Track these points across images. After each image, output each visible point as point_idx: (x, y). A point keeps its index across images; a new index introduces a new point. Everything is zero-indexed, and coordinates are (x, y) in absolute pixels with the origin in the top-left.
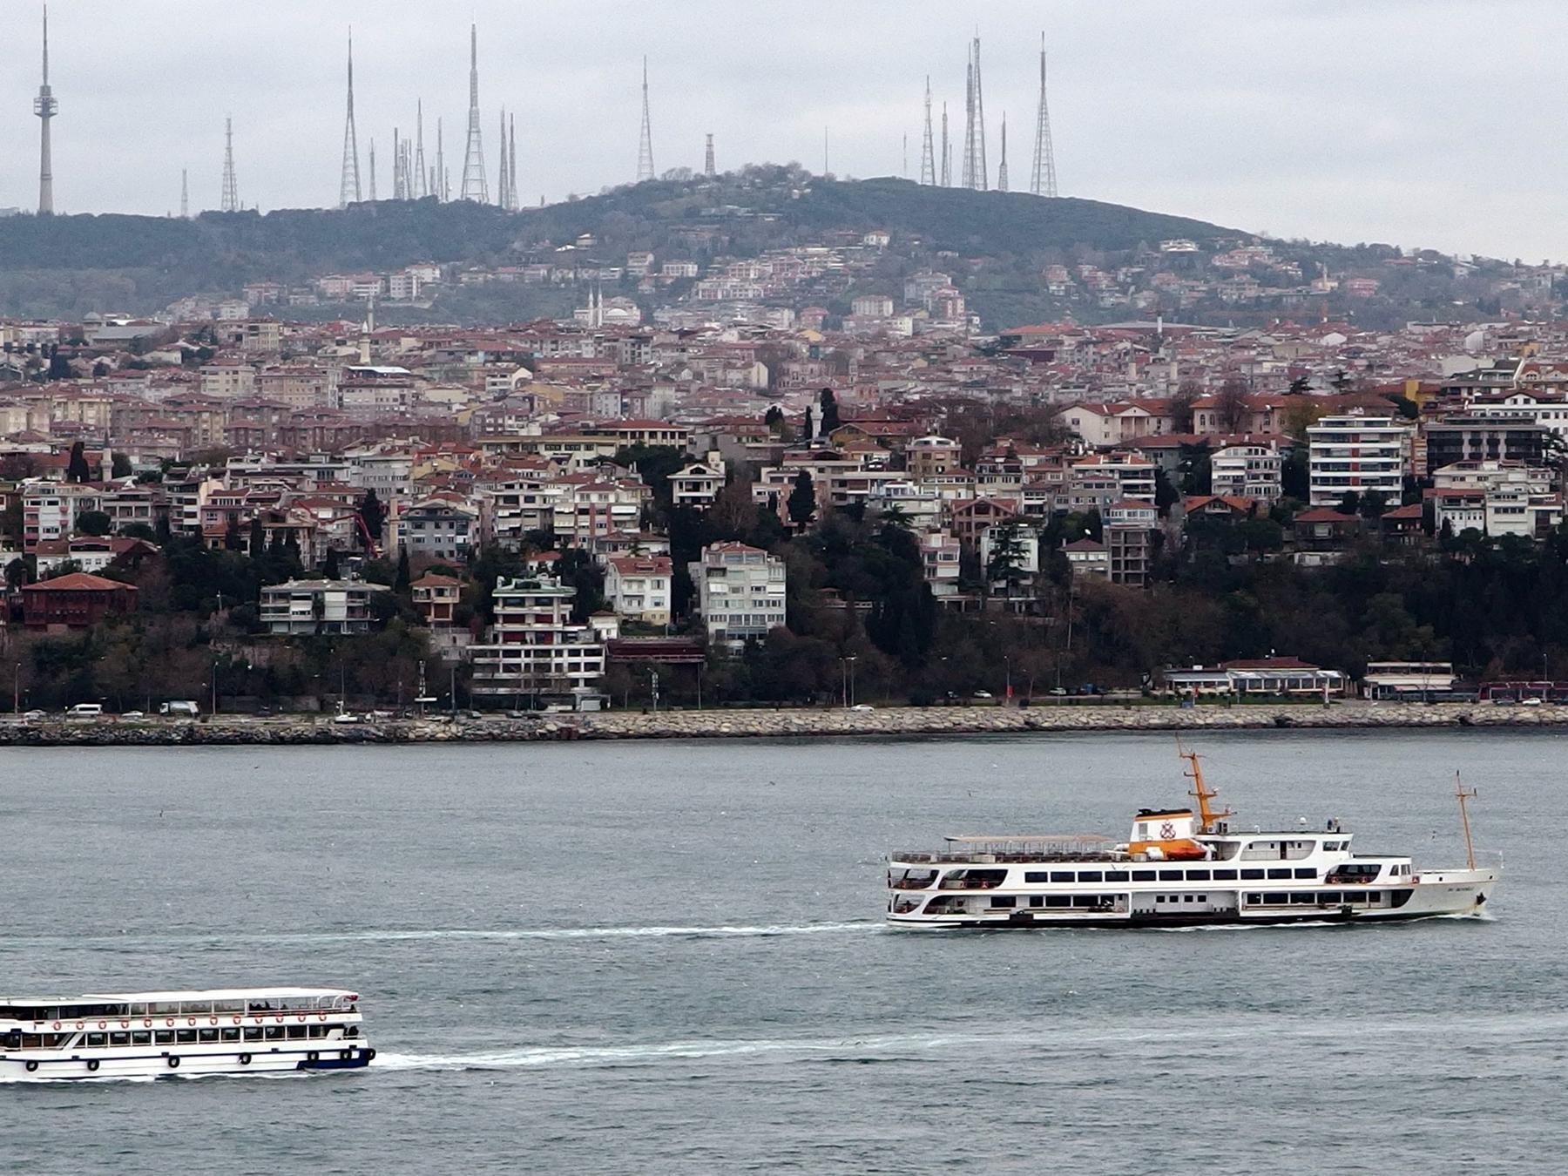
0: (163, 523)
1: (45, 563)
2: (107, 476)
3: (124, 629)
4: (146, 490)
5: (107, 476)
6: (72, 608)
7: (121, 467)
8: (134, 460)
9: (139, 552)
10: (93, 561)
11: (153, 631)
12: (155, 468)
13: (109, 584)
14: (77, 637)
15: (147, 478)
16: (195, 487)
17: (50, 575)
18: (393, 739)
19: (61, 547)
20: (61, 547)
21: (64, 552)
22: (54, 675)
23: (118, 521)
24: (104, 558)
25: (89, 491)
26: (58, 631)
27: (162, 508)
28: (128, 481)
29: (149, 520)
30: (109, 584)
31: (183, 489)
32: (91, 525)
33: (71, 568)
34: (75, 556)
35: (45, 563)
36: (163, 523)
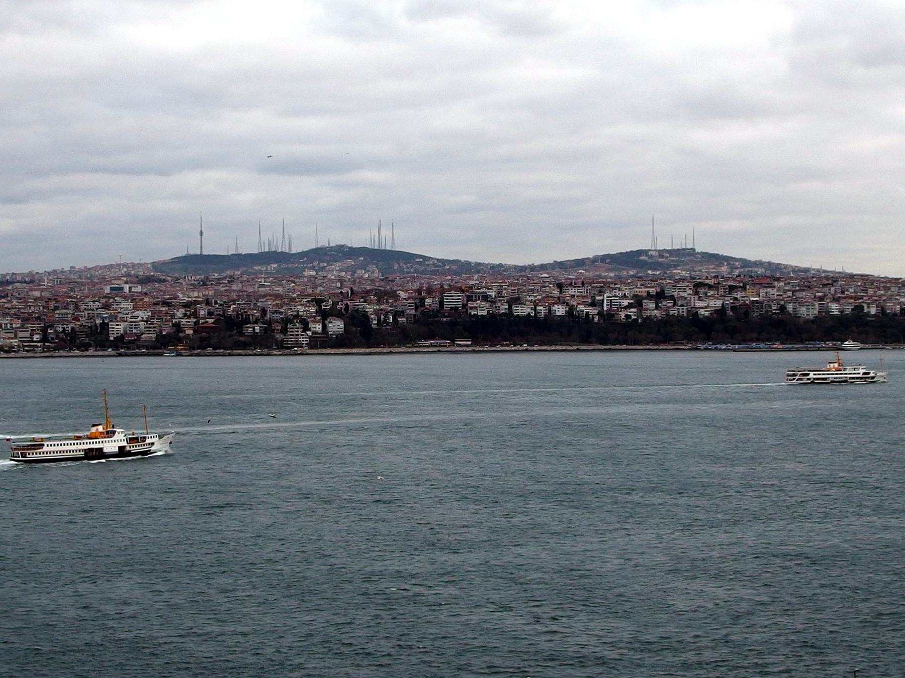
9: (219, 319)
15: (221, 305)
18: (269, 355)
19: (204, 318)
20: (204, 318)
26: (204, 334)
27: (224, 311)
32: (210, 314)
33: (207, 322)
35: (201, 321)
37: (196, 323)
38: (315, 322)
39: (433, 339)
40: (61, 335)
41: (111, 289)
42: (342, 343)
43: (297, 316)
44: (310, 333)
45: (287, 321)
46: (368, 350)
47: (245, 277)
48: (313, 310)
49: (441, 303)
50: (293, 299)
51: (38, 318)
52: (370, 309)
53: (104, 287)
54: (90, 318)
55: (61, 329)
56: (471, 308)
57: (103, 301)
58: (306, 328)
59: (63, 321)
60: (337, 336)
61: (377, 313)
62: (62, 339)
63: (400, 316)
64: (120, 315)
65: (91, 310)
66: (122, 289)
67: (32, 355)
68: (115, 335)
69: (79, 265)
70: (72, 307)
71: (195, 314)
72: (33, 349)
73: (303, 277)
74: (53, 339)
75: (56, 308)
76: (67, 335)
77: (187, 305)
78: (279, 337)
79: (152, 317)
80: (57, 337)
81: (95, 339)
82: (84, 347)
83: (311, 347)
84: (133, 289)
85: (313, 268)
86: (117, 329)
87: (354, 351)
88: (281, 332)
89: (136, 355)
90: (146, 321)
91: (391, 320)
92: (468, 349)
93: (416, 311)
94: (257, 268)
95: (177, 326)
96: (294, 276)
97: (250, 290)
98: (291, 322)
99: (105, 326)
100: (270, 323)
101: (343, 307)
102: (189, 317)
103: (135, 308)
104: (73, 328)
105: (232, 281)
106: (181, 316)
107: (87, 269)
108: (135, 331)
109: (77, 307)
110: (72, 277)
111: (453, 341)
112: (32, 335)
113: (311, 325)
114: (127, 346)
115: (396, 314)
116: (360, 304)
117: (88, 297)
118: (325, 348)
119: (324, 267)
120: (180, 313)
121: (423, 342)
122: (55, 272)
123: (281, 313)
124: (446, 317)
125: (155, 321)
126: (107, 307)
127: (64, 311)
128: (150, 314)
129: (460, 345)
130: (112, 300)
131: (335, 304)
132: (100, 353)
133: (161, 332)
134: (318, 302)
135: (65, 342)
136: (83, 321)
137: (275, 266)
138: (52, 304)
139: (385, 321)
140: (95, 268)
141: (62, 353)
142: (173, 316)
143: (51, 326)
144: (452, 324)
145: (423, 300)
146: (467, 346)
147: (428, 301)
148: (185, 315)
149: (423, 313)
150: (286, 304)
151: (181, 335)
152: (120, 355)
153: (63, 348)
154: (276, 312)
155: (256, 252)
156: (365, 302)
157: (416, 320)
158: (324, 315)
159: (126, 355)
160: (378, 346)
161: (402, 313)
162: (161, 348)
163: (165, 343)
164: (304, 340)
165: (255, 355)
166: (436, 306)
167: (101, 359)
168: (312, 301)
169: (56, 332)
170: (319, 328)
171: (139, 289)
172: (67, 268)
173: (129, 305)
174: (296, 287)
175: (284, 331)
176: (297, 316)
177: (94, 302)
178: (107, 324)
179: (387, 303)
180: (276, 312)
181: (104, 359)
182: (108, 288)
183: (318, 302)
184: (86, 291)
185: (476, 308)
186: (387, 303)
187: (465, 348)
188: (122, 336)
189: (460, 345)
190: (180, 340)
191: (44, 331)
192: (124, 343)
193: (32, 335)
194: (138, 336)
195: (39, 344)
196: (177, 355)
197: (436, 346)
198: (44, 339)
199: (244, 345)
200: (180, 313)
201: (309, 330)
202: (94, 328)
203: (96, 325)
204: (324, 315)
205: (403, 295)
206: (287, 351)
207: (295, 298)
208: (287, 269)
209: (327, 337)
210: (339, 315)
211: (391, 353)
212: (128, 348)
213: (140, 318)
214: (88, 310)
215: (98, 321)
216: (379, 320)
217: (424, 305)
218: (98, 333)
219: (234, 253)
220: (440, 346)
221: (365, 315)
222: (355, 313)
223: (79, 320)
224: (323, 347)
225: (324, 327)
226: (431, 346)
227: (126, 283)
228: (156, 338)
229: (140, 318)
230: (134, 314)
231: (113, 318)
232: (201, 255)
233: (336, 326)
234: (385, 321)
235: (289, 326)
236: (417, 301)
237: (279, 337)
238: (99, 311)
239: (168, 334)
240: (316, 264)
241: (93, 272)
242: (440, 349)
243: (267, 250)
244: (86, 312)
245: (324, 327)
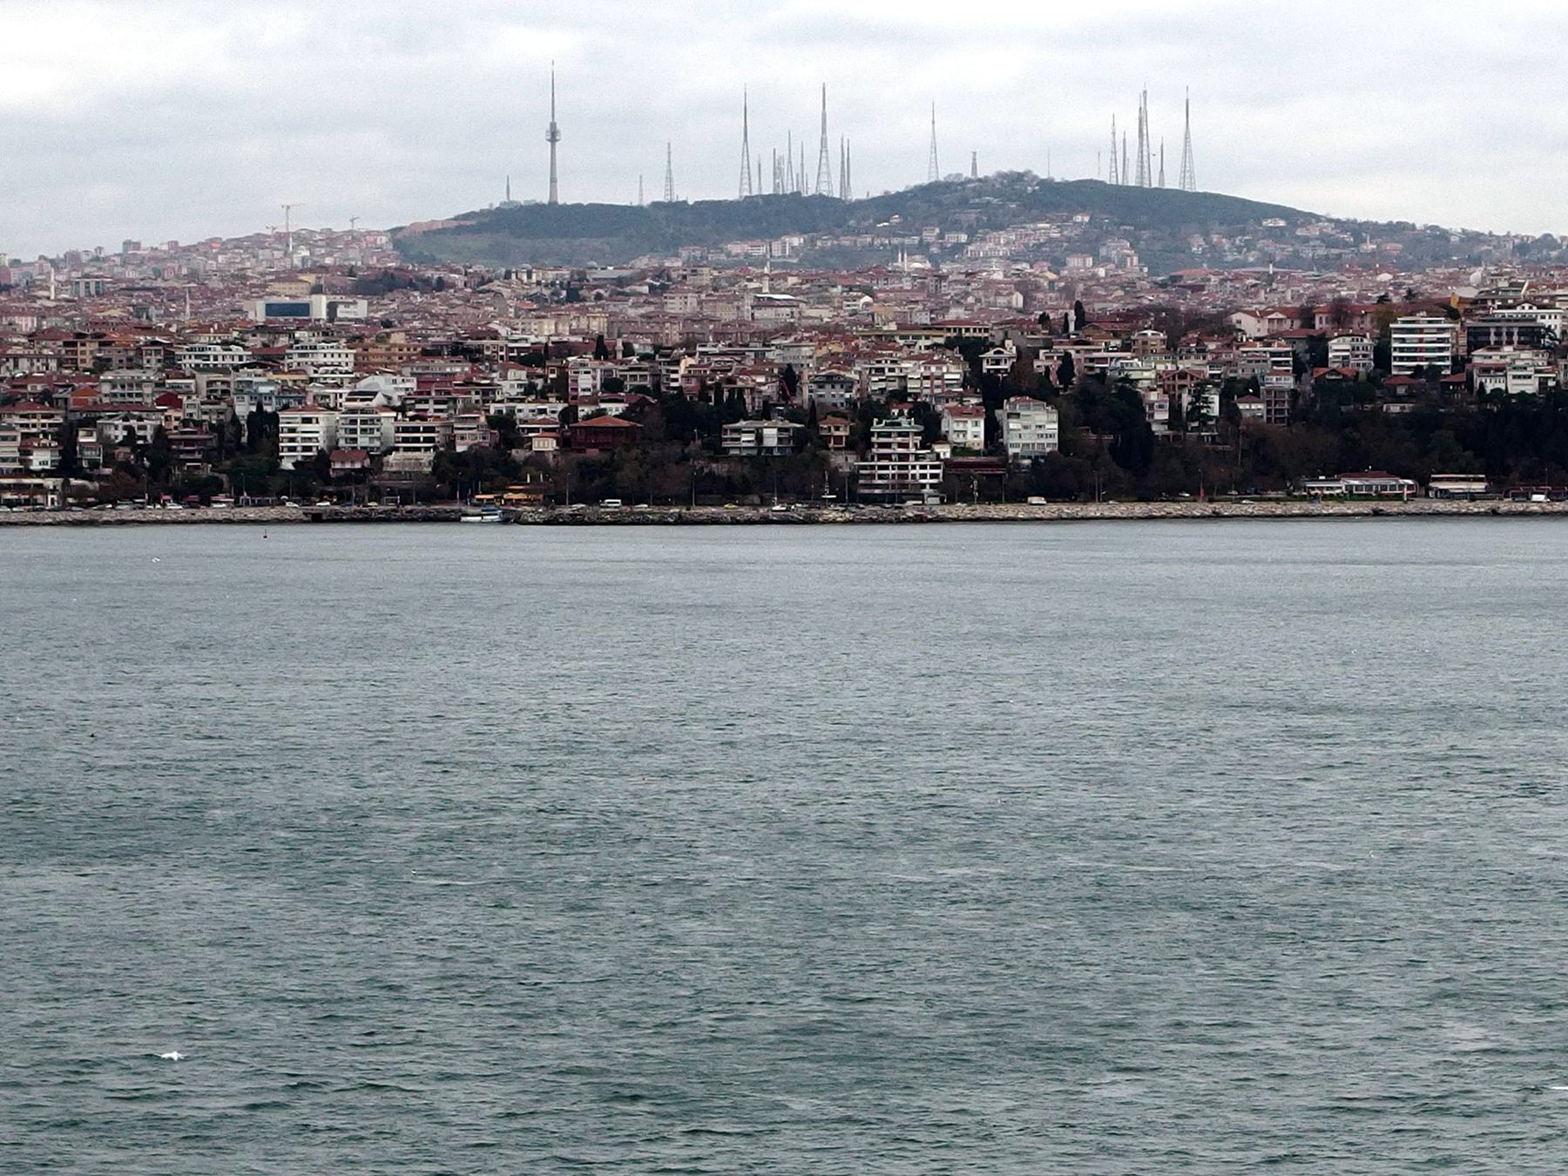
0: (657, 385)
1: (584, 410)
2: (620, 356)
3: (636, 452)
4: (646, 364)
5: (620, 356)
6: (602, 439)
7: (628, 350)
8: (636, 346)
10: (614, 409)
11: (654, 453)
12: (650, 351)
13: (626, 423)
14: (605, 456)
15: (644, 357)
16: (677, 363)
17: (587, 417)
19: (593, 400)
20: (593, 400)
21: (596, 403)
22: (592, 480)
23: (628, 384)
24: (621, 407)
25: (610, 365)
26: (593, 453)
28: (635, 359)
29: (648, 383)
30: (626, 423)
31: (669, 363)
32: (612, 386)
33: (601, 413)
34: (603, 406)
35: (584, 410)
36: (657, 385)
37: (568, 415)
38: (960, 413)
39: (1356, 471)
40: (122, 453)
41: (270, 309)
42: (1061, 481)
43: (901, 395)
44: (944, 451)
45: (866, 412)
46: (1139, 509)
47: (706, 276)
48: (954, 373)
49: (1382, 355)
50: (884, 340)
51: (45, 397)
52: (1145, 372)
53: (245, 305)
54: (217, 396)
55: (121, 434)
56: (1486, 370)
57: (256, 341)
58: (932, 433)
59: (127, 408)
60: (1035, 460)
61: (1170, 384)
62: (125, 466)
63: (1243, 394)
64: (314, 389)
65: (215, 369)
66: (305, 309)
67: (30, 517)
68: (299, 455)
69: (153, 238)
70: (153, 361)
71: (561, 387)
72: (29, 497)
73: (898, 274)
74: (94, 464)
75: (102, 365)
76: (142, 451)
77: (534, 358)
78: (844, 462)
79: (422, 395)
80: (109, 460)
81: (237, 466)
82: (198, 493)
83: (949, 498)
84: (341, 312)
85: (923, 248)
86: (305, 433)
87: (1093, 510)
88: (851, 446)
89: (367, 519)
90: (402, 409)
91: (1215, 410)
92: (1474, 507)
93: (1298, 379)
94: (736, 248)
95: (504, 425)
96: (869, 273)
97: (727, 314)
98: (882, 412)
99: (264, 424)
100: (812, 415)
101: (1055, 365)
102: (542, 396)
103: (364, 366)
104: (159, 431)
105: (664, 288)
106: (514, 392)
107: (179, 252)
108: (363, 441)
109: (170, 361)
110: (131, 274)
111: (1423, 482)
112: (25, 452)
113: (949, 425)
114: (339, 488)
115: (1233, 390)
116: (1108, 355)
117: (203, 329)
118: (997, 500)
119: (959, 248)
120: (512, 382)
121: (1321, 485)
122: (73, 258)
123: (848, 384)
124: (1398, 399)
125: (431, 407)
126: (268, 360)
127: (127, 374)
128: (412, 384)
129: (1446, 495)
130: (283, 340)
131: (1025, 356)
132: (252, 513)
133: (451, 443)
134: (970, 349)
135: (136, 476)
136: (193, 406)
137: (796, 241)
138: (88, 352)
139: (1195, 412)
140: (207, 248)
141: (125, 510)
142: (488, 392)
143: (89, 423)
144: (1419, 424)
145: (1318, 346)
146: (1472, 497)
147: (1339, 347)
148: (529, 389)
149: (1321, 386)
150: (868, 356)
151: (518, 454)
152: (317, 519)
153: (130, 496)
154: (830, 380)
155: (732, 195)
156: (1126, 347)
157: (1297, 410)
158: (993, 393)
159: (335, 519)
160: (1173, 496)
161: (1251, 388)
162: (451, 498)
163: (455, 485)
164: (924, 472)
165: (765, 521)
166: (1364, 364)
167: (261, 529)
168: (950, 344)
169: (106, 444)
170: (973, 432)
171: (361, 309)
172: (113, 248)
173: (341, 356)
174: (876, 307)
175: (860, 443)
176: (901, 395)
177: (226, 344)
178: (274, 418)
179: (1202, 351)
180: (830, 380)
181: (271, 529)
182: (260, 306)
183: (970, 349)
184: (186, 317)
185: (1500, 369)
186: (1202, 351)
187: (1465, 505)
188: (323, 459)
189: (1446, 495)
190: (513, 473)
191: (65, 436)
192: (328, 481)
193: (25, 452)
194: (376, 458)
195: (49, 483)
196: (505, 521)
197: (1367, 498)
198: (67, 466)
199: (729, 490)
200: (512, 382)
201: (943, 439)
202: (229, 432)
203: (235, 419)
204: (993, 393)
205: (1251, 326)
206: (868, 510)
207: (890, 337)
208: (839, 252)
209: (1004, 464)
210: (1041, 391)
211: (1217, 516)
212: (343, 498)
213: (379, 400)
214: (206, 369)
215: (243, 409)
216: (1175, 409)
217: (1324, 361)
218: (240, 446)
219: (660, 197)
220: (1381, 497)
221: (1128, 392)
222: (1094, 387)
223: (178, 405)
224: (989, 497)
225: (994, 430)
226: (1351, 495)
227: (317, 290)
228: (436, 464)
229: (379, 400)
230: (362, 386)
231: (293, 397)
232: (553, 204)
233: (1033, 429)
234: (1195, 412)
235: (877, 427)
236: (1301, 347)
237: (844, 462)
238: (244, 375)
239: (475, 454)
240: (930, 235)
241: (198, 261)
242: (1382, 506)
243: (768, 190)
244: (203, 379)
245: (994, 430)
